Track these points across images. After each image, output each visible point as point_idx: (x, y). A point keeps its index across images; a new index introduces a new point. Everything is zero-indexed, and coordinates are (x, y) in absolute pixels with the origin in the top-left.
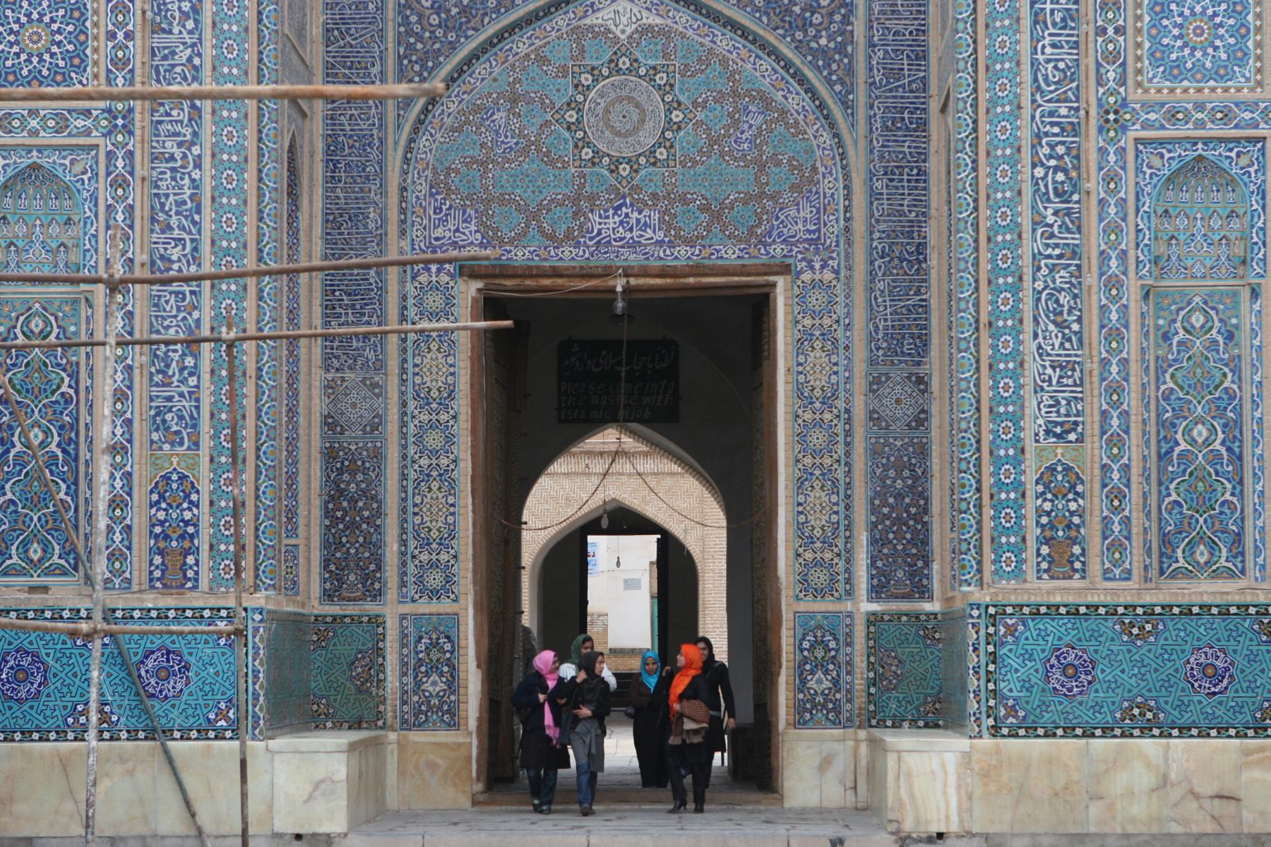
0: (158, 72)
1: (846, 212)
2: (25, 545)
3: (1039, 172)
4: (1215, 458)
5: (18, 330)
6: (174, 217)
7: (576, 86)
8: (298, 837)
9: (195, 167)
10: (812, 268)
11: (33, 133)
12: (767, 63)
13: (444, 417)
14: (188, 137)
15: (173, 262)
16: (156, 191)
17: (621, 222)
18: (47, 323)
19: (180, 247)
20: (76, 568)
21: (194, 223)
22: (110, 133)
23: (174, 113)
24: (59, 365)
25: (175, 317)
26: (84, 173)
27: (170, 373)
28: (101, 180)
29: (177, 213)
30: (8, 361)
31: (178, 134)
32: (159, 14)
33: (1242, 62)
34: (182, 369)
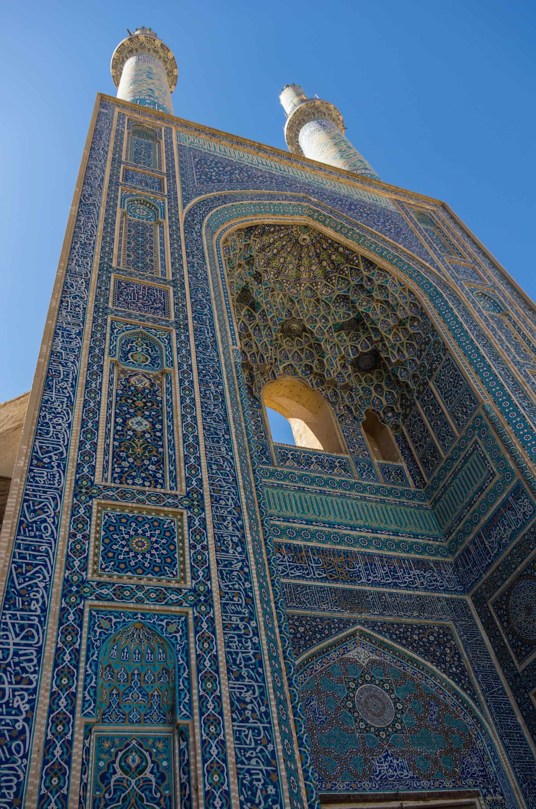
0: (222, 574)
1: (494, 759)
5: (116, 765)
6: (244, 669)
7: (348, 688)
9: (254, 635)
10: (490, 792)
14: (247, 615)
15: (247, 703)
16: (228, 650)
17: (390, 766)
18: (143, 758)
19: (251, 692)
21: (259, 674)
22: (195, 605)
23: (236, 599)
24: (153, 799)
25: (254, 749)
26: (177, 632)
27: (257, 801)
28: (192, 634)
29: (246, 666)
30: (107, 796)
31: (240, 613)
32: (219, 541)
34: (266, 798)
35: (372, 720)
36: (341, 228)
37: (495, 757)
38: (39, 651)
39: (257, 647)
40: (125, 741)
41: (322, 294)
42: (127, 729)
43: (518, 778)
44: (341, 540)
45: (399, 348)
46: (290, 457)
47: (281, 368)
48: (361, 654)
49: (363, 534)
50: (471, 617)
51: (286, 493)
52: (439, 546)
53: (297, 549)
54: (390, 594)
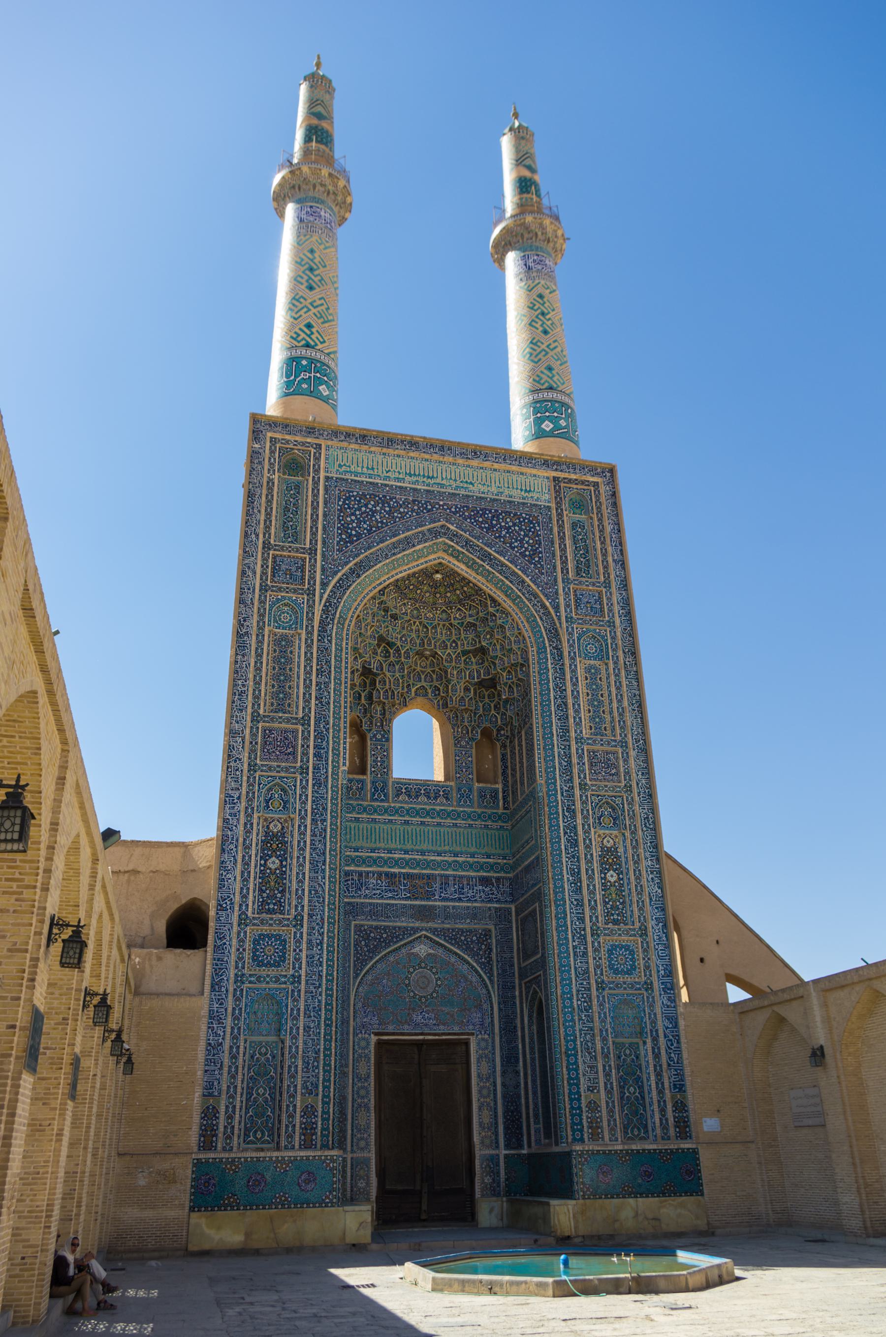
2: (256, 1132)
3: (579, 1003)
4: (637, 1098)
8: (354, 1245)
11: (268, 983)
12: (466, 966)
13: (366, 1084)
18: (267, 1049)
20: (273, 1141)
33: (635, 970)
35: (419, 991)
36: (472, 564)
37: (492, 1014)
38: (226, 1010)
39: (319, 1001)
40: (260, 1043)
41: (454, 619)
42: (261, 1038)
43: (500, 1027)
44: (428, 864)
45: (510, 686)
46: (404, 791)
47: (413, 690)
48: (422, 950)
49: (446, 858)
50: (510, 922)
51: (394, 827)
52: (505, 864)
53: (394, 875)
54: (454, 907)
